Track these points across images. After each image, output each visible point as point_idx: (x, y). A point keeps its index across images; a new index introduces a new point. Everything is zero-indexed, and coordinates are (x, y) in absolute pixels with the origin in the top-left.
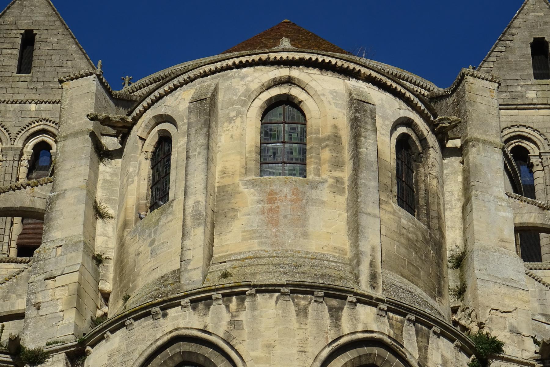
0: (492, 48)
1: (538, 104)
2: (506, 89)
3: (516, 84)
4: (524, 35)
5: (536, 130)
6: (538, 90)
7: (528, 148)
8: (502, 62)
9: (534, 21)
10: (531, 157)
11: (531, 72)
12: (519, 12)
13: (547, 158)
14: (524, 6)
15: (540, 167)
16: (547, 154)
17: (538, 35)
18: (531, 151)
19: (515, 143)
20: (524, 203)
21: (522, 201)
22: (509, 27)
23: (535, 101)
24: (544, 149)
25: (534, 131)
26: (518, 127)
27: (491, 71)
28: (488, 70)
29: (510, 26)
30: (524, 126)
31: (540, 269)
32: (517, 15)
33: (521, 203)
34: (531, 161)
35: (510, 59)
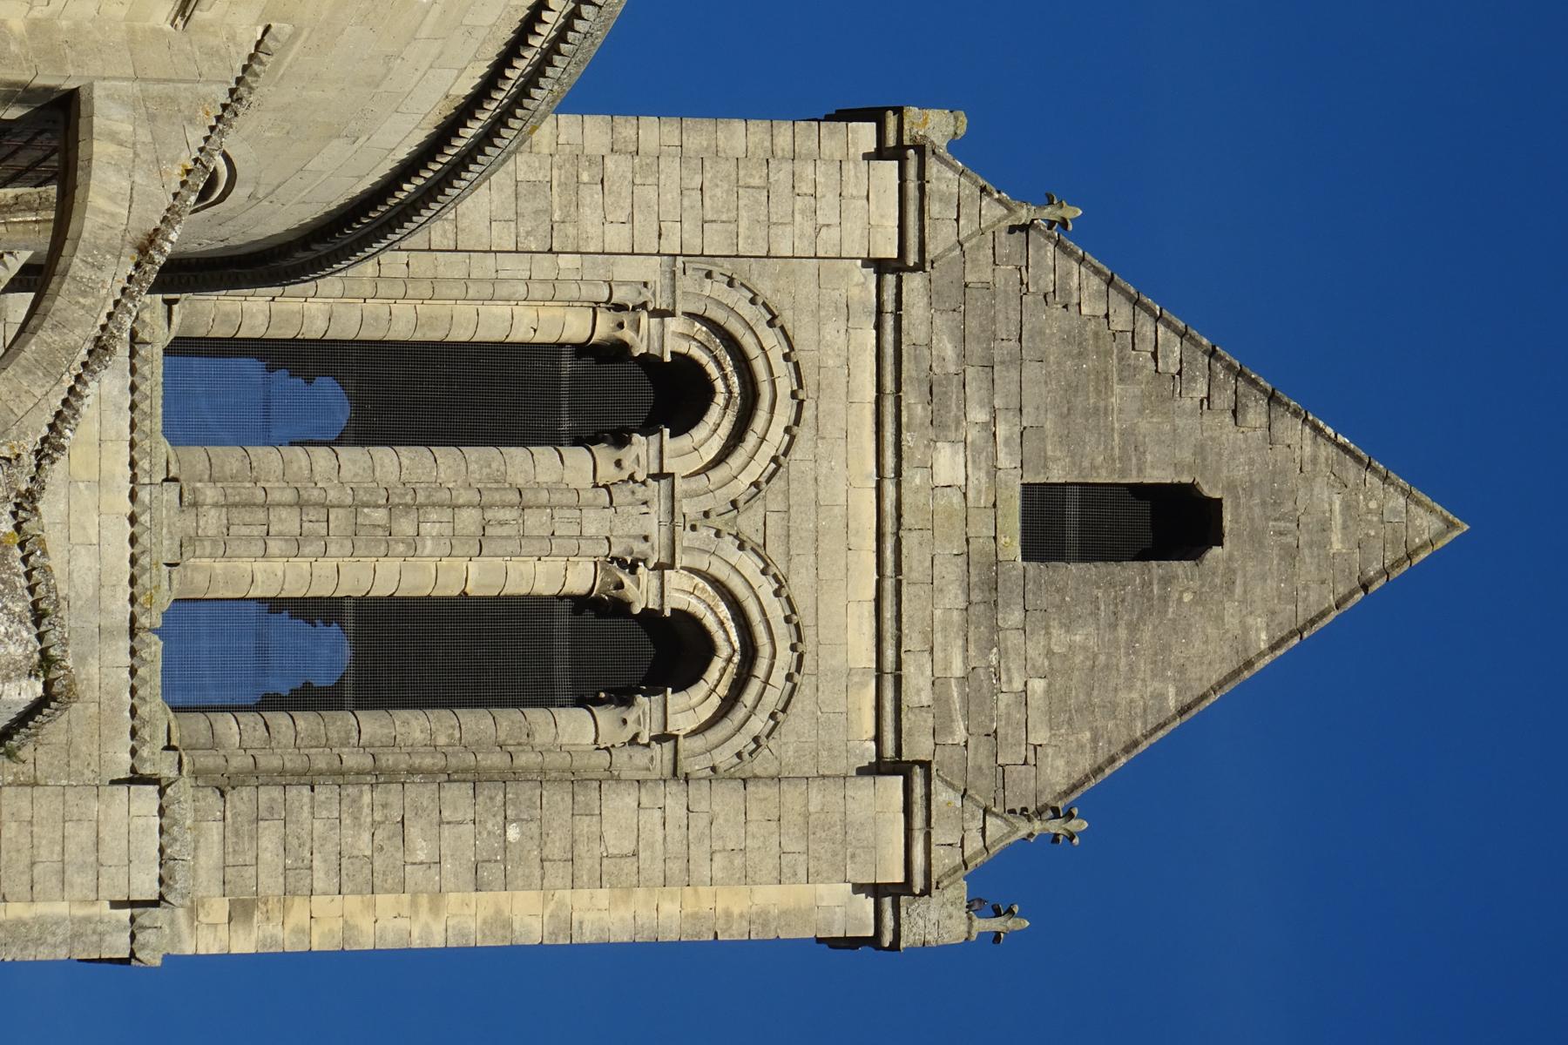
0: (1174, 319)
1: (898, 485)
2: (975, 361)
3: (998, 403)
4: (1232, 457)
5: (779, 466)
6: (970, 495)
7: (700, 432)
8: (1108, 353)
9: (1301, 507)
10: (654, 439)
11: (1057, 475)
12: (1344, 448)
13: (645, 503)
14: (1375, 471)
15: (607, 472)
16: (664, 505)
17: (1235, 521)
18: (685, 441)
19: (725, 377)
20: (179, 179)
21: (188, 172)
22: (1272, 398)
23: (914, 478)
24: (689, 495)
25: (775, 459)
26: (794, 395)
27: (1065, 307)
28: (1070, 294)
29: (1280, 402)
30: (797, 422)
31: (133, 426)
32: (1329, 438)
33: (178, 170)
34: (636, 437)
35: (1117, 388)
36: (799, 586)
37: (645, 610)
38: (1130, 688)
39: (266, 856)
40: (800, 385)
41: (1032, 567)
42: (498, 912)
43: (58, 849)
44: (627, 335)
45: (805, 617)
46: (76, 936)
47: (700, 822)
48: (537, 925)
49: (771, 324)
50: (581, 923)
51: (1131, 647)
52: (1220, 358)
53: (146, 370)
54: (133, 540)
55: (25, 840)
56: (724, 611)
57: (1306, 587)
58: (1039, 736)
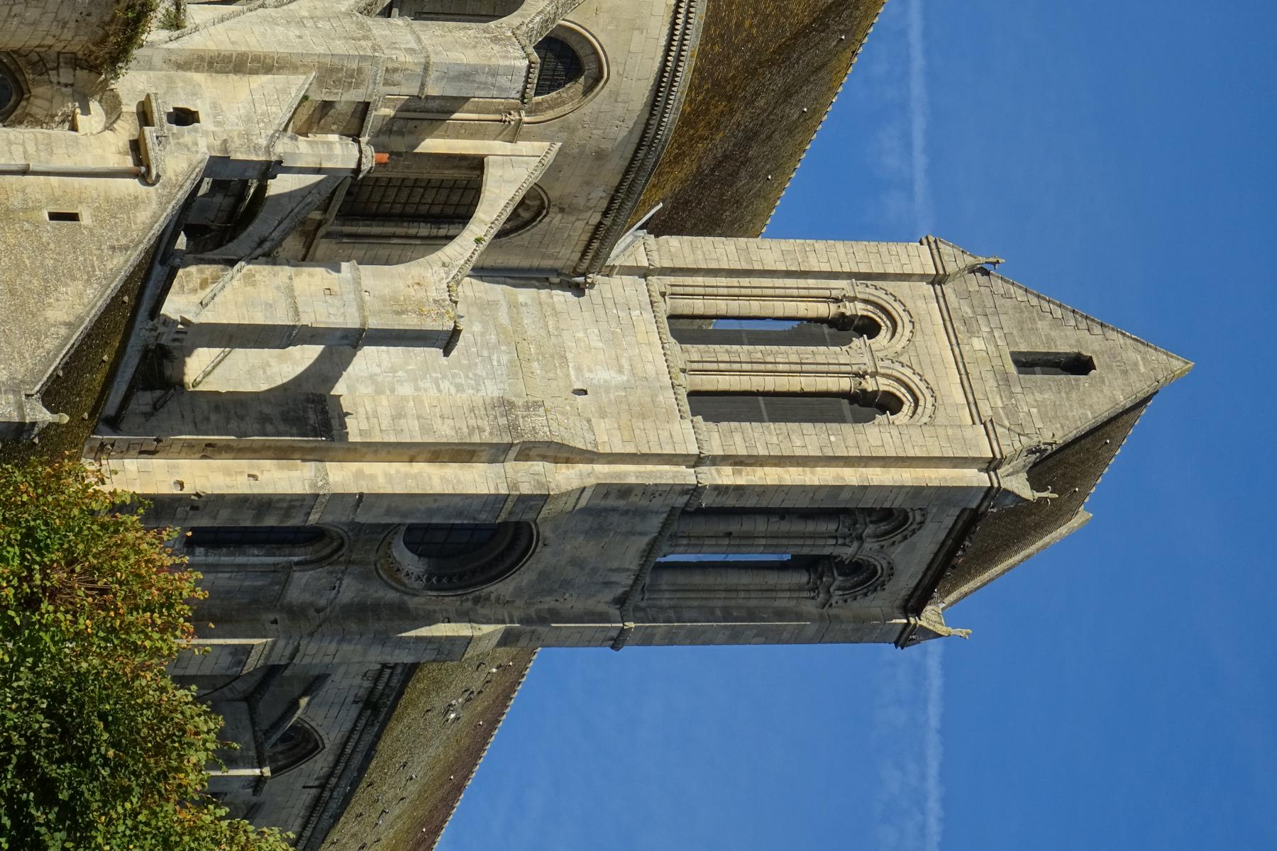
8: (1032, 312)
10: (861, 339)
14: (1151, 347)
16: (869, 354)
19: (884, 322)
23: (965, 348)
32: (1129, 337)
36: (929, 377)
37: (852, 341)
38: (1072, 411)
39: (737, 443)
40: (911, 317)
41: (1021, 376)
42: (838, 475)
43: (657, 438)
44: (842, 310)
45: (932, 384)
46: (674, 477)
47: (906, 437)
48: (854, 479)
49: (895, 300)
50: (872, 479)
51: (1068, 399)
52: (1077, 313)
53: (662, 325)
54: (666, 361)
55: (644, 435)
56: (903, 390)
57: (1134, 382)
58: (1040, 425)
